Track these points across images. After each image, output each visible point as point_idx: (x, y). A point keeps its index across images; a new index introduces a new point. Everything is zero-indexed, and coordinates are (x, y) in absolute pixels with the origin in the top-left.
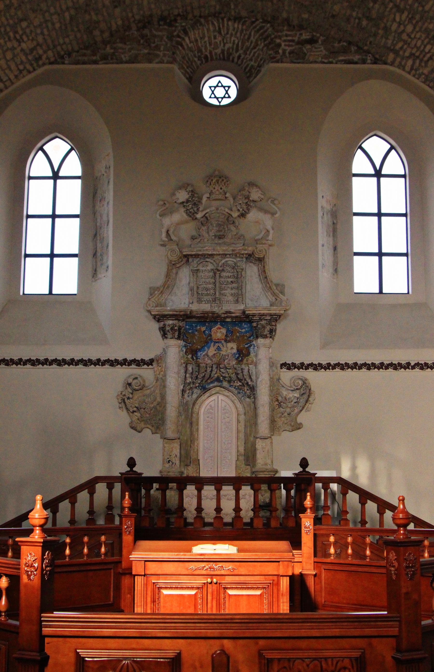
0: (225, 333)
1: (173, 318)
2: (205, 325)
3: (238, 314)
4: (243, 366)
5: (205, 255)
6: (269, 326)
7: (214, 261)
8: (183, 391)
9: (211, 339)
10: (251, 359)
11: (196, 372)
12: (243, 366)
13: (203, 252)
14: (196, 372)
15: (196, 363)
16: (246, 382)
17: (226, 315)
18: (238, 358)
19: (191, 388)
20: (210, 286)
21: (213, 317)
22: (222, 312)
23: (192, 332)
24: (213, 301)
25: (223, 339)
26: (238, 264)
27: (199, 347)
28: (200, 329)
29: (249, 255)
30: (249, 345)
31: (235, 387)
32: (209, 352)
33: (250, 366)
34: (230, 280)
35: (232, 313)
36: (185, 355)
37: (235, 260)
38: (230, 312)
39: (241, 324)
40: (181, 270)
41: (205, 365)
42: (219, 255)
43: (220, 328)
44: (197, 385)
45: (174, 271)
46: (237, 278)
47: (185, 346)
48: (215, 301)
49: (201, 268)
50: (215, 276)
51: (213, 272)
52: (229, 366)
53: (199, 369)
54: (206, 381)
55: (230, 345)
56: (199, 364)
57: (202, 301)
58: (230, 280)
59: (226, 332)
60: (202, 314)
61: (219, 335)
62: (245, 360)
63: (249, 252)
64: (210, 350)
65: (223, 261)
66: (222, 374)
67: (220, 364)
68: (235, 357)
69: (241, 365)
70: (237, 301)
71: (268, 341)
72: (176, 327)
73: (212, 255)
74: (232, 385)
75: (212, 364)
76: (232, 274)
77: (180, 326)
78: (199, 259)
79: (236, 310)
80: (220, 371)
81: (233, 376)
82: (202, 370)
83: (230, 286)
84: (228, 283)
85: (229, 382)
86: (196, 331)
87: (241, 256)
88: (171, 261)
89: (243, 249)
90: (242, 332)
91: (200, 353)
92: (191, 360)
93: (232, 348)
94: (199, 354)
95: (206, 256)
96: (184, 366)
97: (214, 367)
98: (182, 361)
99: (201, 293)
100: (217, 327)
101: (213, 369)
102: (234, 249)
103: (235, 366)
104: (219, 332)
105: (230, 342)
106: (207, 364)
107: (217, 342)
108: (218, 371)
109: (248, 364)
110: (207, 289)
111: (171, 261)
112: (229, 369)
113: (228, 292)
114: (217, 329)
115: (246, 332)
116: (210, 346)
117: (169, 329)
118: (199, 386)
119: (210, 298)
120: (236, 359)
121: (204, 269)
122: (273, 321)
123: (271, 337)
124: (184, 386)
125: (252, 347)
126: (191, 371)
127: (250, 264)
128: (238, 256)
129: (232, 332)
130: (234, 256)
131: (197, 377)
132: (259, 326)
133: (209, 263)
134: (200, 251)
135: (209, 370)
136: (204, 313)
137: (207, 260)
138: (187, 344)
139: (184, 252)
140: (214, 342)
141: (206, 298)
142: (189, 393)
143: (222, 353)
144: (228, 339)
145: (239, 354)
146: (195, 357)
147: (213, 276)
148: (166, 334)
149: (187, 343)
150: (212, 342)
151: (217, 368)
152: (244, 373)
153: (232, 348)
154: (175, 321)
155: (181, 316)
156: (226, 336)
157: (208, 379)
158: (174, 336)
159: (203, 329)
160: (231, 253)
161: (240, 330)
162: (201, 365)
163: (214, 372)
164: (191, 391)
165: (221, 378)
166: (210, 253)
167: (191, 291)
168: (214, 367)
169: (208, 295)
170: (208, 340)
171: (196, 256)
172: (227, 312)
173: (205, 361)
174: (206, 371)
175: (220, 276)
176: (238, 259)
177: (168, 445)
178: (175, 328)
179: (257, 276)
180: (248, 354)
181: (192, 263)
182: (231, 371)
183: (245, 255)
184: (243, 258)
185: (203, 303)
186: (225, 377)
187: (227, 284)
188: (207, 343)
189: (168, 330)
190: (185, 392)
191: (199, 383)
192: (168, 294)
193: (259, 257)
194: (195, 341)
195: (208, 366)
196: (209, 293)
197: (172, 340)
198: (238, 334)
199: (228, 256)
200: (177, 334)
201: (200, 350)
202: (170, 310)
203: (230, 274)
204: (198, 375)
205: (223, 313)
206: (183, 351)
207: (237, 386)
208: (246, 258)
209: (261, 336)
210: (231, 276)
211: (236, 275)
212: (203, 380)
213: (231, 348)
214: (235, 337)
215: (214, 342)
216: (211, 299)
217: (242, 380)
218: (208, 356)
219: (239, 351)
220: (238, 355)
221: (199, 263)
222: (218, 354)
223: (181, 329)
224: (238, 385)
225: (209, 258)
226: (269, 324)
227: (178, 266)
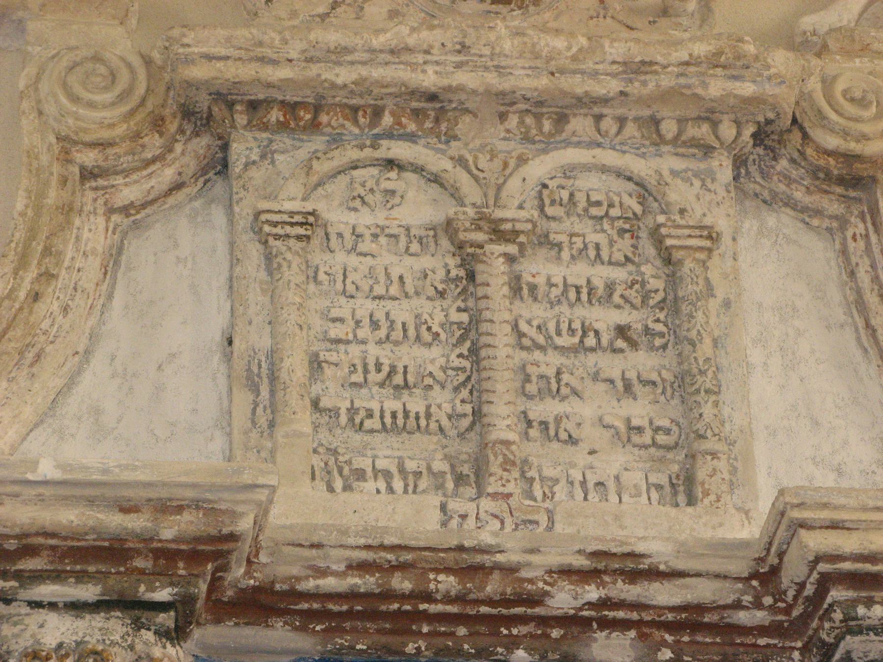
1: (81, 577)
3: (702, 591)
5: (377, 113)
7: (461, 161)
13: (364, 71)
17: (593, 593)
20: (434, 358)
22: (554, 559)
24: (460, 479)
26: (673, 196)
29: (758, 137)
34: (605, 318)
35: (654, 574)
37: (640, 167)
38: (637, 569)
40: (156, 234)
42: (504, 103)
45: (93, 233)
46: (672, 304)
48: (480, 473)
49: (338, 217)
50: (471, 276)
51: (445, 243)
57: (360, 475)
58: (605, 318)
60: (363, 567)
63: (770, 89)
65: (540, 168)
70: (685, 488)
73: (434, 109)
76: (620, 274)
78: (318, 143)
79: (683, 549)
83: (612, 366)
84: (585, 340)
87: (692, 131)
88: (67, 144)
89: (714, 62)
95: (387, 120)
99: (345, 405)
102: (638, 54)
110: (397, 381)
111: (67, 144)
113: (590, 409)
119: (422, 451)
121: (365, 219)
127: (771, 220)
128: (669, 128)
130: (631, 129)
133: (409, 176)
134: (338, 55)
136: (388, 558)
137: (399, 150)
139: (189, 61)
141: (386, 451)
147: (448, 280)
154: (98, 621)
155: (166, 557)
160: (614, 86)
166: (429, 79)
167: (255, 390)
169: (398, 425)
171: (300, 113)
172: (602, 565)
175: (516, 287)
176: (669, 163)
179: (839, 314)
181: (257, 175)
183: (728, 131)
184: (708, 151)
185: (370, 485)
187: (581, 348)
192: (28, 413)
193: (854, 147)
196: (416, 405)
199: (580, 125)
202: (70, 489)
203: (601, 275)
205: (566, 572)
208: (739, 162)
210: (610, 287)
211: (654, 284)
216: (439, 465)
221: (322, 167)
225: (412, 138)
227: (129, 192)
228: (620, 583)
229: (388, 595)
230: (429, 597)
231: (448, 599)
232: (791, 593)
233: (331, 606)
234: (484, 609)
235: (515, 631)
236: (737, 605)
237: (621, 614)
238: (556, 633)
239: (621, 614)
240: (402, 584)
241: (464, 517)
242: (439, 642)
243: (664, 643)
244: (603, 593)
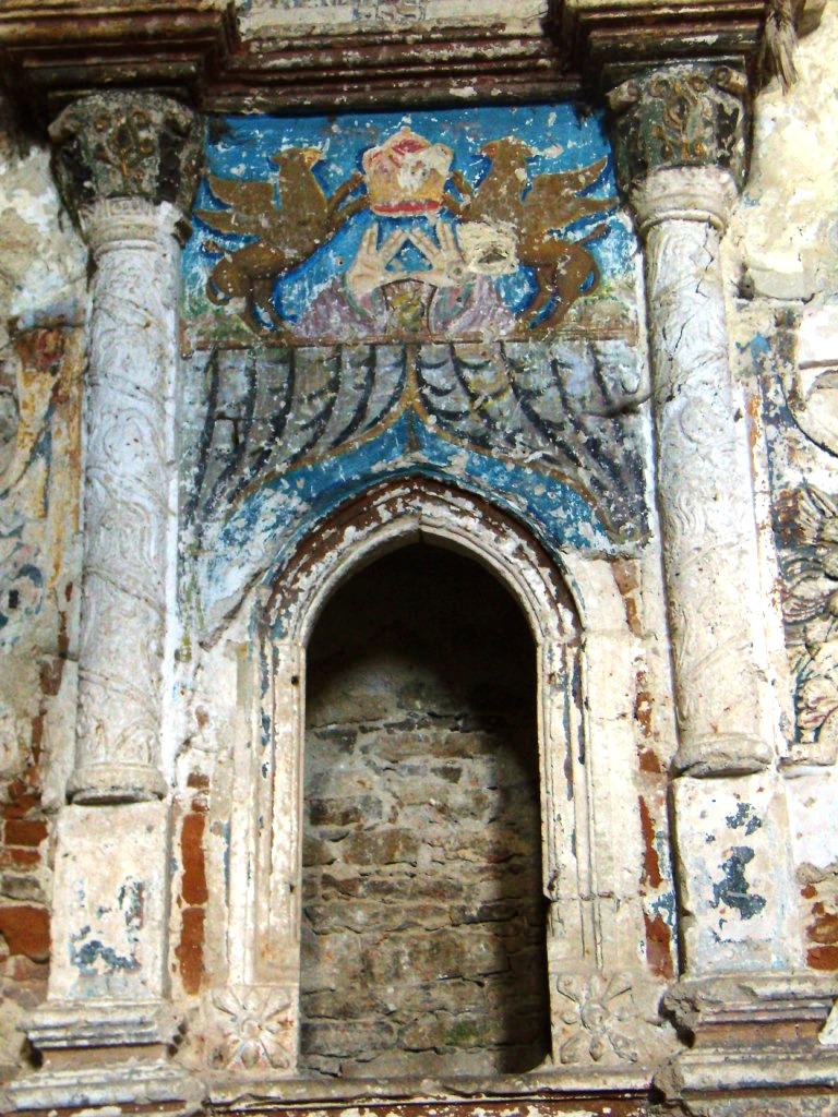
0: (445, 173)
2: (327, 131)
3: (515, 47)
4: (562, 350)
6: (711, 92)
8: (195, 507)
9: (360, 210)
10: (606, 306)
11: (274, 391)
12: (562, 350)
14: (274, 391)
15: (271, 346)
16: (584, 438)
18: (529, 302)
19: (244, 484)
21: (369, 74)
23: (249, 178)
25: (432, 204)
27: (290, 253)
28: (292, 153)
30: (590, 228)
31: (518, 469)
32: (350, 277)
33: (607, 347)
36: (206, 301)
39: (540, 125)
41: (326, 352)
43: (413, 147)
44: (280, 468)
47: (208, 255)
52: (472, 355)
53: (292, 377)
54: (337, 443)
55: (477, 236)
56: (292, 348)
59: (452, 168)
61: (408, 183)
62: (572, 311)
64: (357, 269)
66: (434, 399)
67: (419, 345)
68: (509, 298)
69: (549, 343)
71: (710, 184)
72: (146, 125)
74: (502, 461)
75: (373, 347)
77: (171, 123)
80: (421, 382)
81: (506, 408)
82: (310, 383)
85: (480, 442)
86: (274, 167)
90: (546, 164)
91: (297, 287)
92: (244, 326)
93: (493, 255)
94: (291, 291)
96: (202, 363)
97: (386, 359)
98: (193, 339)
100: (398, 138)
101: (380, 372)
103: (514, 349)
104: (409, 163)
105: (480, 220)
106: (339, 347)
107: (398, 221)
108: (411, 383)
109: (589, 338)
112: (477, 368)
114: (399, 148)
115: (571, 158)
116: (357, 246)
117: (104, 138)
118: (289, 476)
120: (515, 309)
122: (735, 65)
123: (724, 162)
124: (199, 480)
125: (610, 242)
126: (244, 391)
129: (487, 160)
131: (279, 423)
132: (647, 100)
135: (352, 377)
138: (220, 241)
140: (378, 220)
142: (229, 514)
143: (429, 278)
144: (466, 200)
145: (535, 283)
146: (269, 307)
148: (88, 173)
149: (217, 233)
150: (366, 224)
151: (402, 363)
152: (568, 390)
153: (493, 255)
156: (454, 184)
157: (349, 430)
158: (138, 182)
159: (315, 151)
161: (535, 151)
162: (305, 353)
163: (382, 393)
164: (242, 506)
165: (432, 419)
168: (386, 359)
170: (342, 211)
173: (327, 326)
174: (335, 385)
177: (87, 843)
178: (143, 135)
180: (590, 278)
182: (486, 376)
186: (454, 416)
188: (334, 225)
189: (100, 148)
190: (209, 511)
191: (295, 459)
194: (264, 223)
195: (346, 358)
197: (123, 202)
198: (521, 174)
200: (151, 170)
201: (294, 268)
204: (287, 410)
206: (195, 278)
207: (533, 464)
209: (665, 156)
212: (316, 437)
213: (480, 251)
214: (503, 190)
215: (378, 220)
217: (560, 426)
218: (344, 299)
219: (537, 265)
220: (523, 291)
222: (407, 287)
223: (179, 146)
224: (538, 455)
226: (713, 81)
228: (462, 48)
229: (320, 67)
230: (344, 66)
231: (355, 66)
232: (569, 43)
233: (285, 77)
234: (380, 71)
235: (401, 85)
236: (536, 56)
237: (465, 67)
238: (427, 84)
239: (465, 67)
240: (328, 59)
241: (368, 16)
242: (356, 96)
243: (495, 85)
244: (451, 54)
